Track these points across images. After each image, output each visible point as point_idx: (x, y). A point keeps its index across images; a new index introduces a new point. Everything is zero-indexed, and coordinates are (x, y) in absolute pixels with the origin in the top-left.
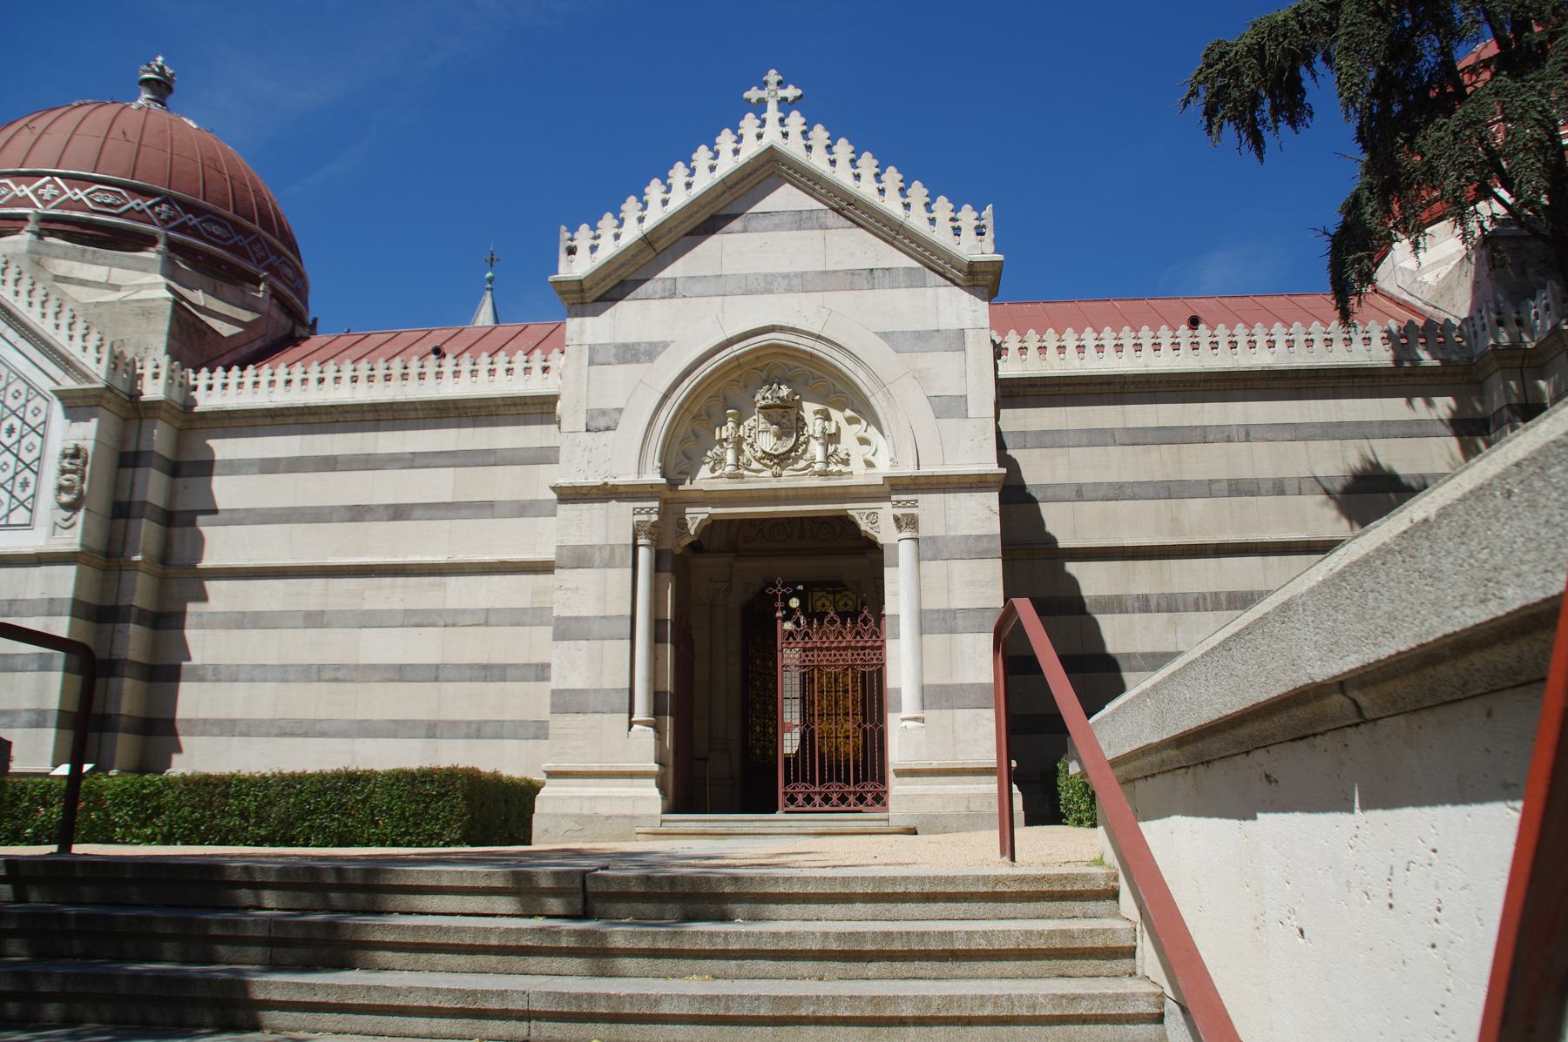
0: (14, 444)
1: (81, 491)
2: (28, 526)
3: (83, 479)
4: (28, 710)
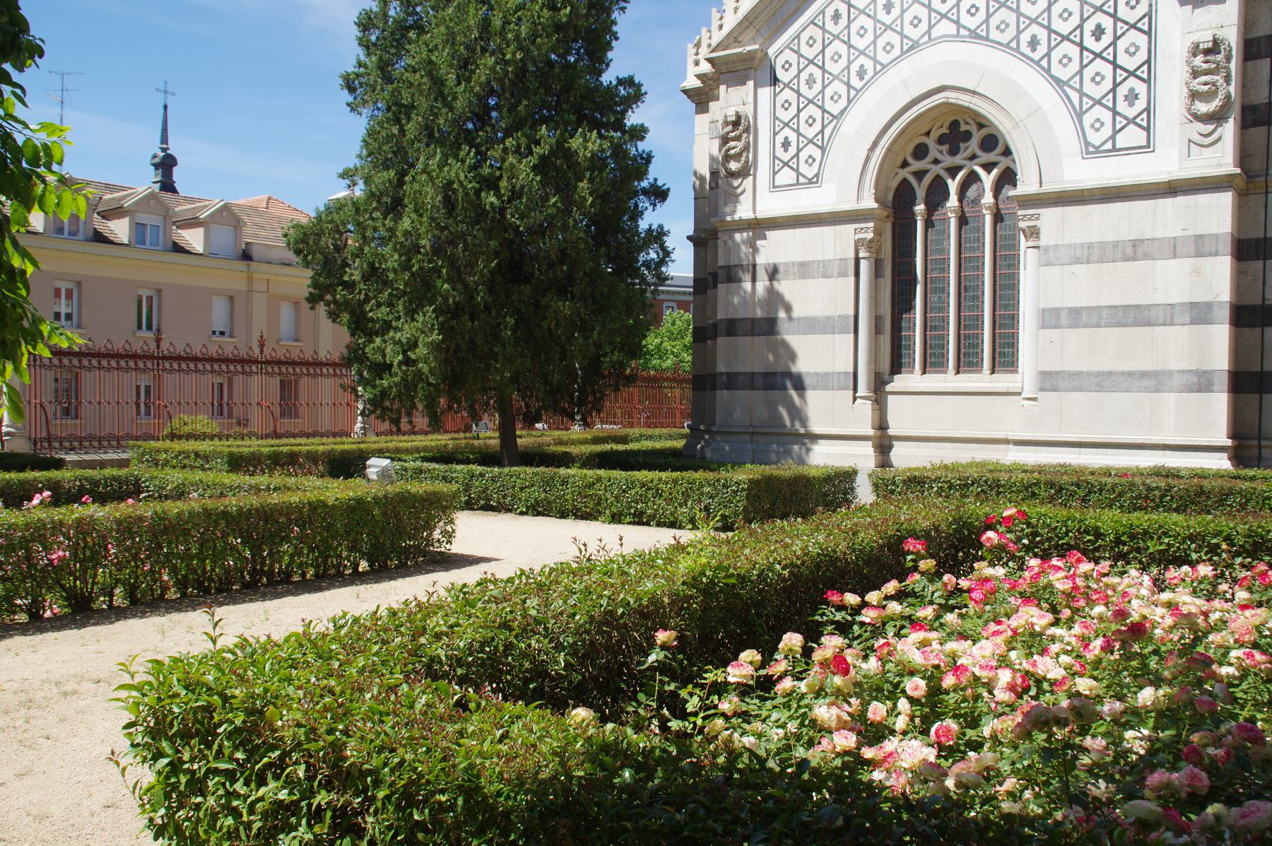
0: (1106, 48)
1: (1228, 96)
2: (1148, 147)
3: (1227, 79)
4: (1183, 372)
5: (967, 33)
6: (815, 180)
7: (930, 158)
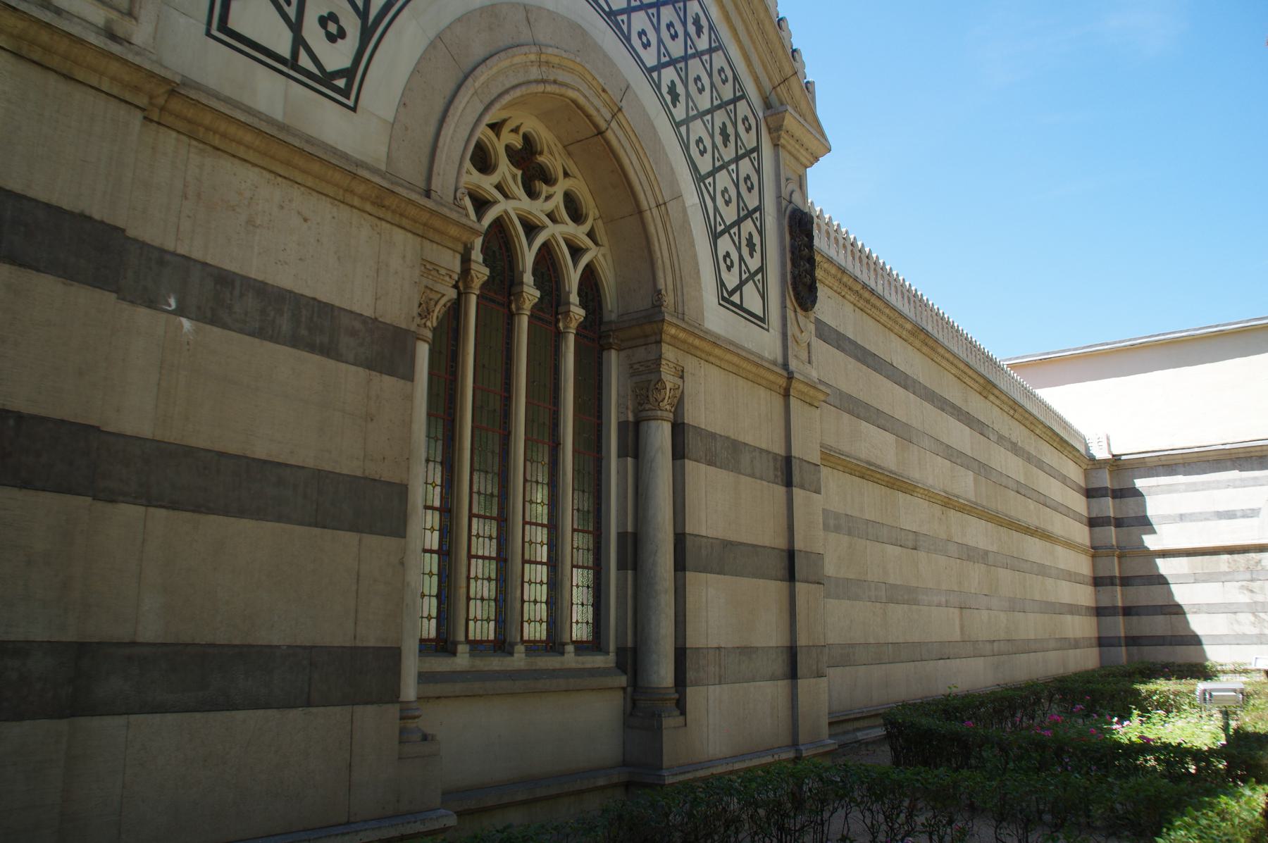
5: (607, 9)
6: (341, 83)
7: (495, 178)
